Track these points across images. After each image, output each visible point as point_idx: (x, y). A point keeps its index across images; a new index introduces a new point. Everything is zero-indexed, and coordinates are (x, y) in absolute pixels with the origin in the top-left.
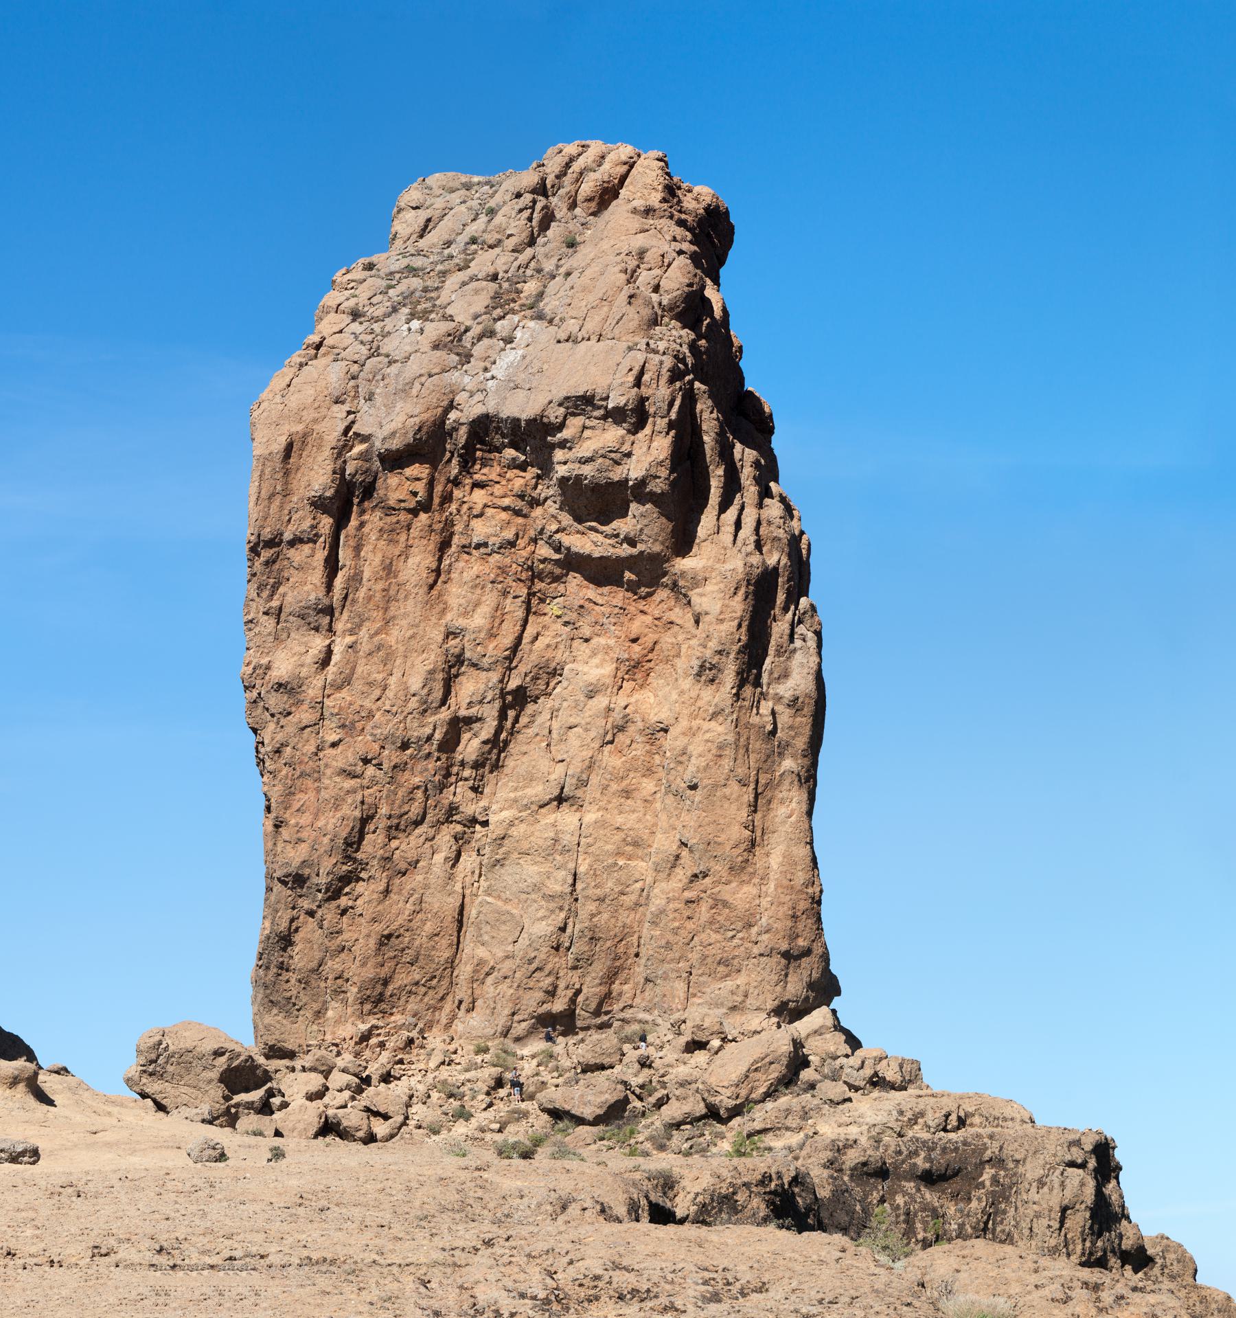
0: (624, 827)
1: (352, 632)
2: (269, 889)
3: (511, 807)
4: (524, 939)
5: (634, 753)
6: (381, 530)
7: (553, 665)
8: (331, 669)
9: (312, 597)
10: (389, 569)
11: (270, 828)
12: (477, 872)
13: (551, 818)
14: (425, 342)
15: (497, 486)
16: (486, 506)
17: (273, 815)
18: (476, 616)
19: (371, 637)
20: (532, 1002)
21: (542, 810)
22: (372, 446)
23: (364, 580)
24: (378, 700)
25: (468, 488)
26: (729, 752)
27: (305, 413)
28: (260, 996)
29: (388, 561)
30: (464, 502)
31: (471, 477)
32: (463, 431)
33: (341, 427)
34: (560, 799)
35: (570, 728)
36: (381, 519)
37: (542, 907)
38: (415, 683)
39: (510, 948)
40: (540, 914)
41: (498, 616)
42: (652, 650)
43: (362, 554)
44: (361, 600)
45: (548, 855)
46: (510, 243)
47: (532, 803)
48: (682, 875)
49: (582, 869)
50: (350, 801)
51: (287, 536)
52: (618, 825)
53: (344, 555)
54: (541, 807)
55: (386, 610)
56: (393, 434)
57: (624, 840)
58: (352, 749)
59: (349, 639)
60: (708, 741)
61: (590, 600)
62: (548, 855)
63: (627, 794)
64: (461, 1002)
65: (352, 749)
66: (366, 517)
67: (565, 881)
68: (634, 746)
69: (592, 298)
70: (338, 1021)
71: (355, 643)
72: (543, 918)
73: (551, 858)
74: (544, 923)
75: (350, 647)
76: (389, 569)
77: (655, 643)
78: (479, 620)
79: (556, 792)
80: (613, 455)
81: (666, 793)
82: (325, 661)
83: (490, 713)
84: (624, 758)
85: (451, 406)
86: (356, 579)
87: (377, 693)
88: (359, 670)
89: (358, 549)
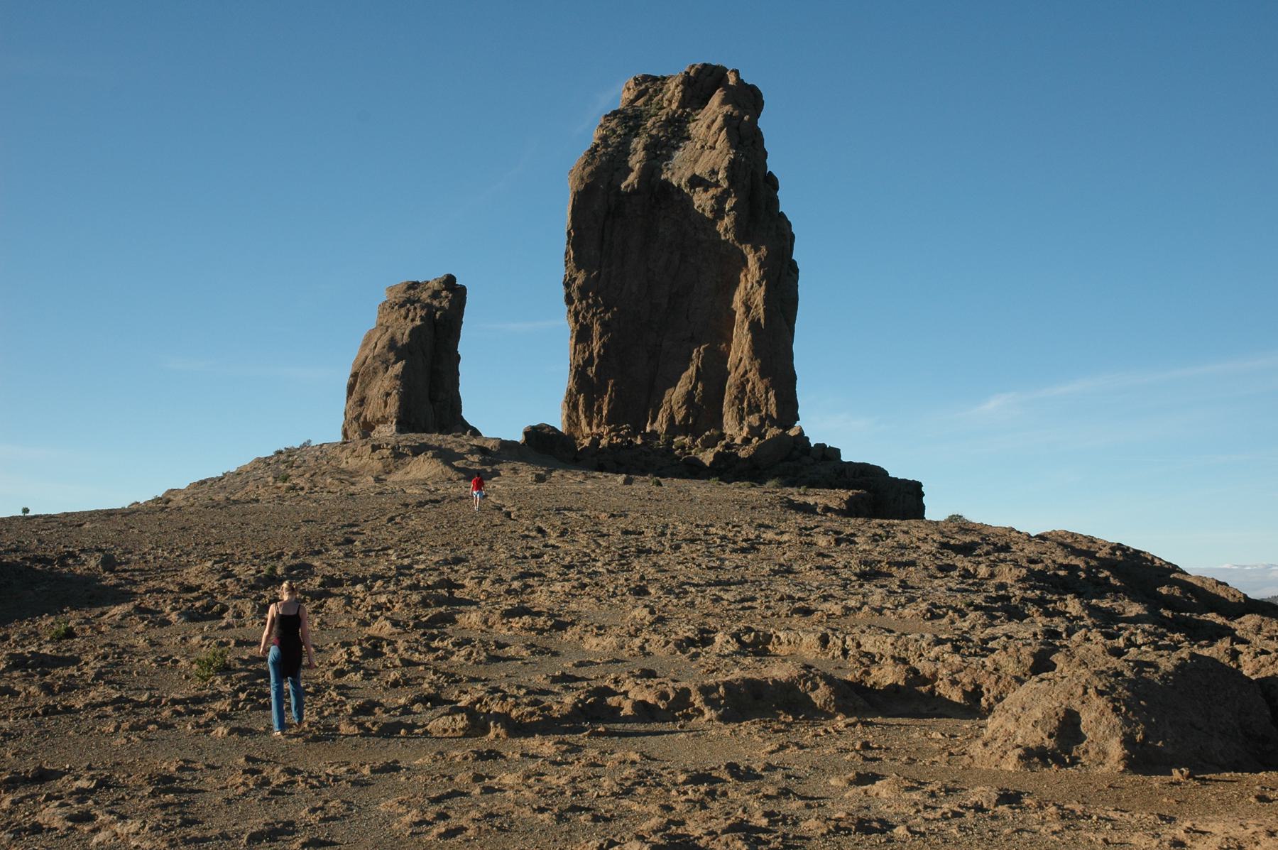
2: (571, 370)
11: (573, 346)
14: (640, 147)
17: (574, 340)
20: (678, 418)
26: (762, 321)
28: (565, 414)
46: (674, 106)
48: (741, 370)
56: (629, 185)
69: (712, 132)
70: (598, 426)
81: (736, 336)
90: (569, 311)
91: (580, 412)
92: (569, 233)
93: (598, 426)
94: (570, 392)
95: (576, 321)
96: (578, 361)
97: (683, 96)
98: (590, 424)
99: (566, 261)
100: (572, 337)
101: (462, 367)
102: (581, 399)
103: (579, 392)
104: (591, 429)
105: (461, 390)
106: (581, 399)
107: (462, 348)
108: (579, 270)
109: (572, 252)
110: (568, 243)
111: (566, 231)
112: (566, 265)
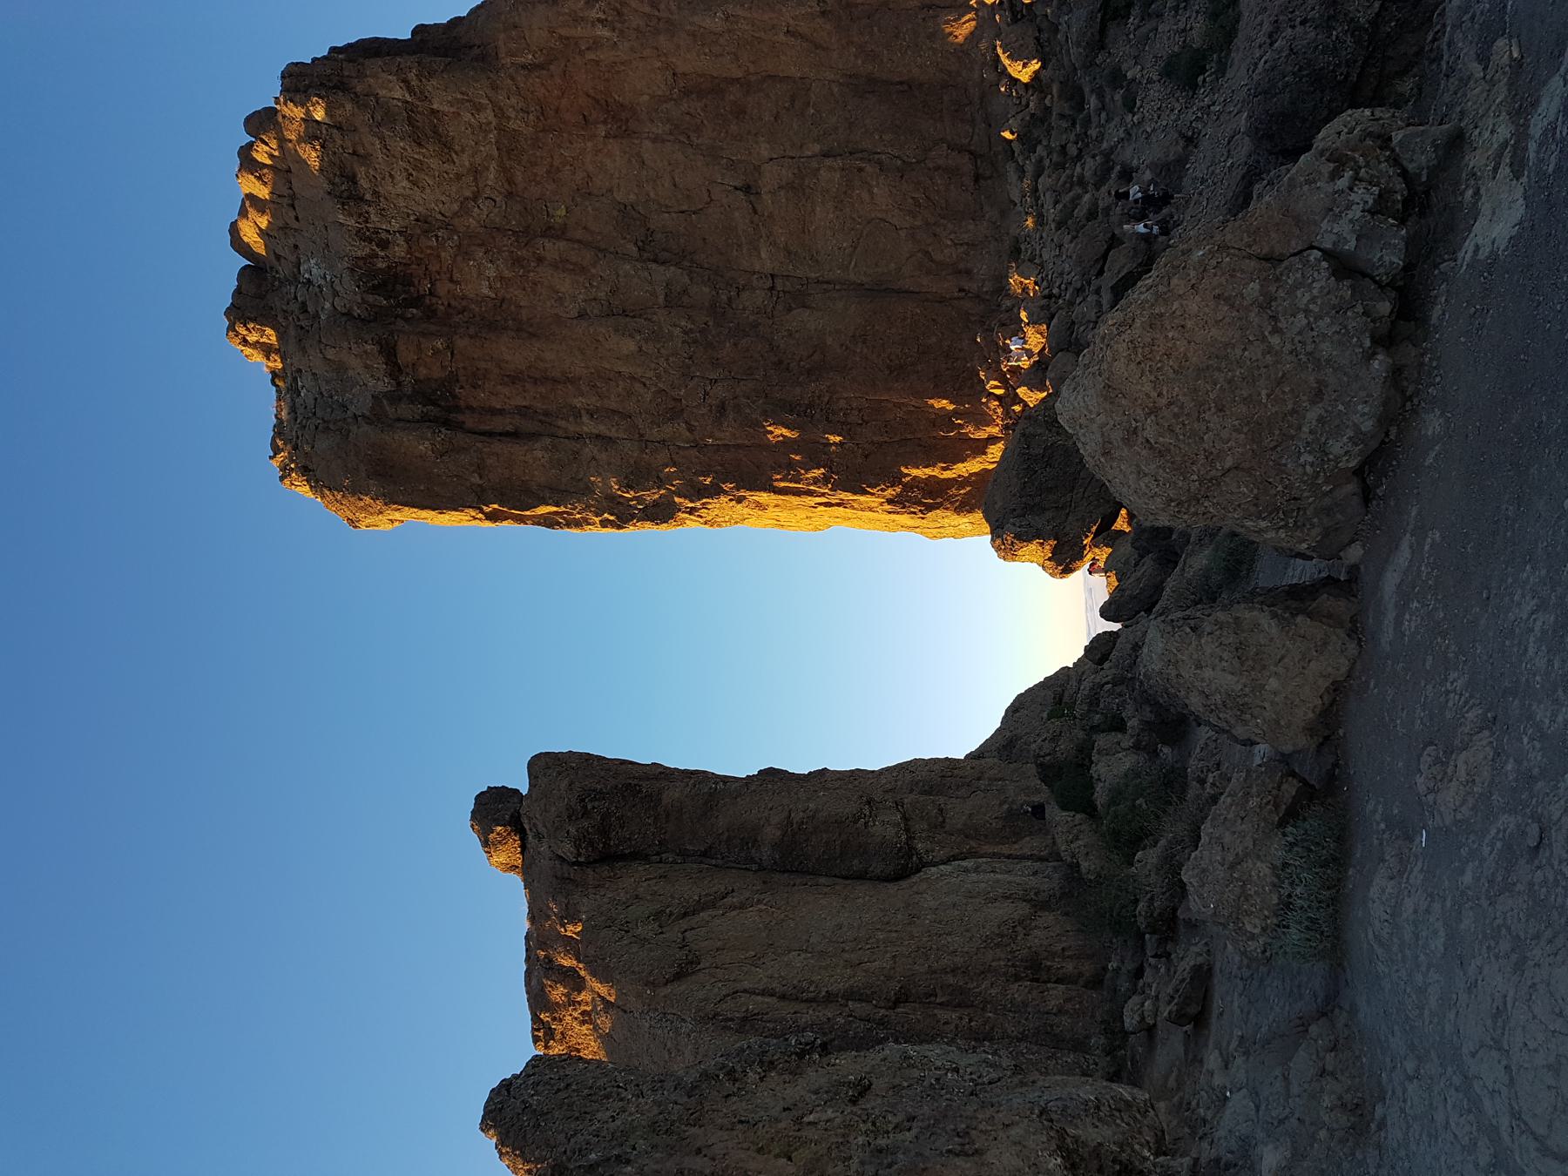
0: (775, 112)
1: (578, 415)
3: (757, 249)
4: (893, 216)
5: (699, 110)
6: (474, 388)
7: (615, 213)
8: (613, 433)
9: (539, 454)
10: (514, 379)
12: (825, 286)
13: (767, 198)
15: (430, 267)
16: (451, 280)
17: (763, 497)
18: (563, 290)
19: (582, 395)
21: (759, 208)
22: (385, 395)
23: (524, 404)
24: (645, 385)
25: (434, 300)
27: (349, 465)
29: (506, 379)
30: (449, 305)
31: (424, 296)
32: (370, 298)
33: (366, 428)
34: (747, 189)
35: (675, 185)
36: (462, 387)
37: (859, 195)
38: (629, 346)
39: (903, 234)
40: (865, 196)
41: (561, 265)
42: (597, 101)
43: (498, 407)
44: (544, 407)
45: (804, 194)
47: (752, 222)
49: (817, 148)
50: (748, 411)
51: (476, 479)
52: (772, 119)
53: (499, 424)
54: (755, 212)
55: (555, 381)
56: (367, 367)
57: (788, 109)
58: (695, 410)
59: (585, 419)
60: (679, 8)
61: (548, 172)
62: (804, 194)
63: (740, 112)
64: (961, 290)
65: (695, 410)
66: (462, 403)
67: (831, 169)
68: (692, 111)
71: (588, 411)
72: (871, 193)
73: (807, 191)
74: (875, 190)
75: (592, 416)
76: (514, 379)
77: (589, 96)
78: (565, 284)
79: (741, 195)
80: (378, 117)
82: (604, 441)
83: (662, 274)
84: (705, 122)
85: (348, 314)
86: (523, 411)
87: (637, 386)
88: (613, 406)
89: (494, 412)
90: (692, 511)
91: (948, 475)
92: (493, 517)
93: (983, 420)
94: (899, 503)
95: (715, 491)
96: (816, 481)
97: (254, 320)
98: (980, 448)
99: (568, 525)
100: (760, 506)
101: (800, 764)
102: (915, 472)
103: (896, 479)
104: (992, 440)
105: (874, 765)
106: (915, 472)
107: (742, 766)
108: (588, 490)
109: (543, 510)
110: (521, 520)
111: (488, 524)
112: (578, 524)
